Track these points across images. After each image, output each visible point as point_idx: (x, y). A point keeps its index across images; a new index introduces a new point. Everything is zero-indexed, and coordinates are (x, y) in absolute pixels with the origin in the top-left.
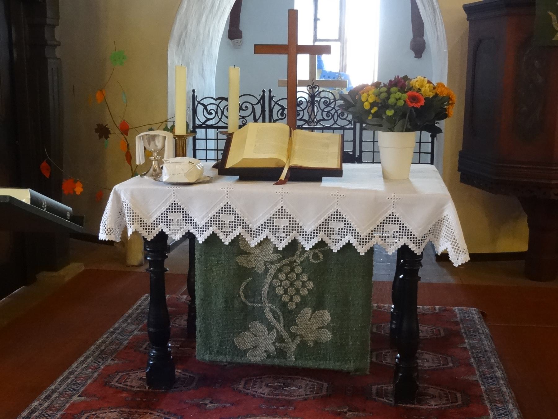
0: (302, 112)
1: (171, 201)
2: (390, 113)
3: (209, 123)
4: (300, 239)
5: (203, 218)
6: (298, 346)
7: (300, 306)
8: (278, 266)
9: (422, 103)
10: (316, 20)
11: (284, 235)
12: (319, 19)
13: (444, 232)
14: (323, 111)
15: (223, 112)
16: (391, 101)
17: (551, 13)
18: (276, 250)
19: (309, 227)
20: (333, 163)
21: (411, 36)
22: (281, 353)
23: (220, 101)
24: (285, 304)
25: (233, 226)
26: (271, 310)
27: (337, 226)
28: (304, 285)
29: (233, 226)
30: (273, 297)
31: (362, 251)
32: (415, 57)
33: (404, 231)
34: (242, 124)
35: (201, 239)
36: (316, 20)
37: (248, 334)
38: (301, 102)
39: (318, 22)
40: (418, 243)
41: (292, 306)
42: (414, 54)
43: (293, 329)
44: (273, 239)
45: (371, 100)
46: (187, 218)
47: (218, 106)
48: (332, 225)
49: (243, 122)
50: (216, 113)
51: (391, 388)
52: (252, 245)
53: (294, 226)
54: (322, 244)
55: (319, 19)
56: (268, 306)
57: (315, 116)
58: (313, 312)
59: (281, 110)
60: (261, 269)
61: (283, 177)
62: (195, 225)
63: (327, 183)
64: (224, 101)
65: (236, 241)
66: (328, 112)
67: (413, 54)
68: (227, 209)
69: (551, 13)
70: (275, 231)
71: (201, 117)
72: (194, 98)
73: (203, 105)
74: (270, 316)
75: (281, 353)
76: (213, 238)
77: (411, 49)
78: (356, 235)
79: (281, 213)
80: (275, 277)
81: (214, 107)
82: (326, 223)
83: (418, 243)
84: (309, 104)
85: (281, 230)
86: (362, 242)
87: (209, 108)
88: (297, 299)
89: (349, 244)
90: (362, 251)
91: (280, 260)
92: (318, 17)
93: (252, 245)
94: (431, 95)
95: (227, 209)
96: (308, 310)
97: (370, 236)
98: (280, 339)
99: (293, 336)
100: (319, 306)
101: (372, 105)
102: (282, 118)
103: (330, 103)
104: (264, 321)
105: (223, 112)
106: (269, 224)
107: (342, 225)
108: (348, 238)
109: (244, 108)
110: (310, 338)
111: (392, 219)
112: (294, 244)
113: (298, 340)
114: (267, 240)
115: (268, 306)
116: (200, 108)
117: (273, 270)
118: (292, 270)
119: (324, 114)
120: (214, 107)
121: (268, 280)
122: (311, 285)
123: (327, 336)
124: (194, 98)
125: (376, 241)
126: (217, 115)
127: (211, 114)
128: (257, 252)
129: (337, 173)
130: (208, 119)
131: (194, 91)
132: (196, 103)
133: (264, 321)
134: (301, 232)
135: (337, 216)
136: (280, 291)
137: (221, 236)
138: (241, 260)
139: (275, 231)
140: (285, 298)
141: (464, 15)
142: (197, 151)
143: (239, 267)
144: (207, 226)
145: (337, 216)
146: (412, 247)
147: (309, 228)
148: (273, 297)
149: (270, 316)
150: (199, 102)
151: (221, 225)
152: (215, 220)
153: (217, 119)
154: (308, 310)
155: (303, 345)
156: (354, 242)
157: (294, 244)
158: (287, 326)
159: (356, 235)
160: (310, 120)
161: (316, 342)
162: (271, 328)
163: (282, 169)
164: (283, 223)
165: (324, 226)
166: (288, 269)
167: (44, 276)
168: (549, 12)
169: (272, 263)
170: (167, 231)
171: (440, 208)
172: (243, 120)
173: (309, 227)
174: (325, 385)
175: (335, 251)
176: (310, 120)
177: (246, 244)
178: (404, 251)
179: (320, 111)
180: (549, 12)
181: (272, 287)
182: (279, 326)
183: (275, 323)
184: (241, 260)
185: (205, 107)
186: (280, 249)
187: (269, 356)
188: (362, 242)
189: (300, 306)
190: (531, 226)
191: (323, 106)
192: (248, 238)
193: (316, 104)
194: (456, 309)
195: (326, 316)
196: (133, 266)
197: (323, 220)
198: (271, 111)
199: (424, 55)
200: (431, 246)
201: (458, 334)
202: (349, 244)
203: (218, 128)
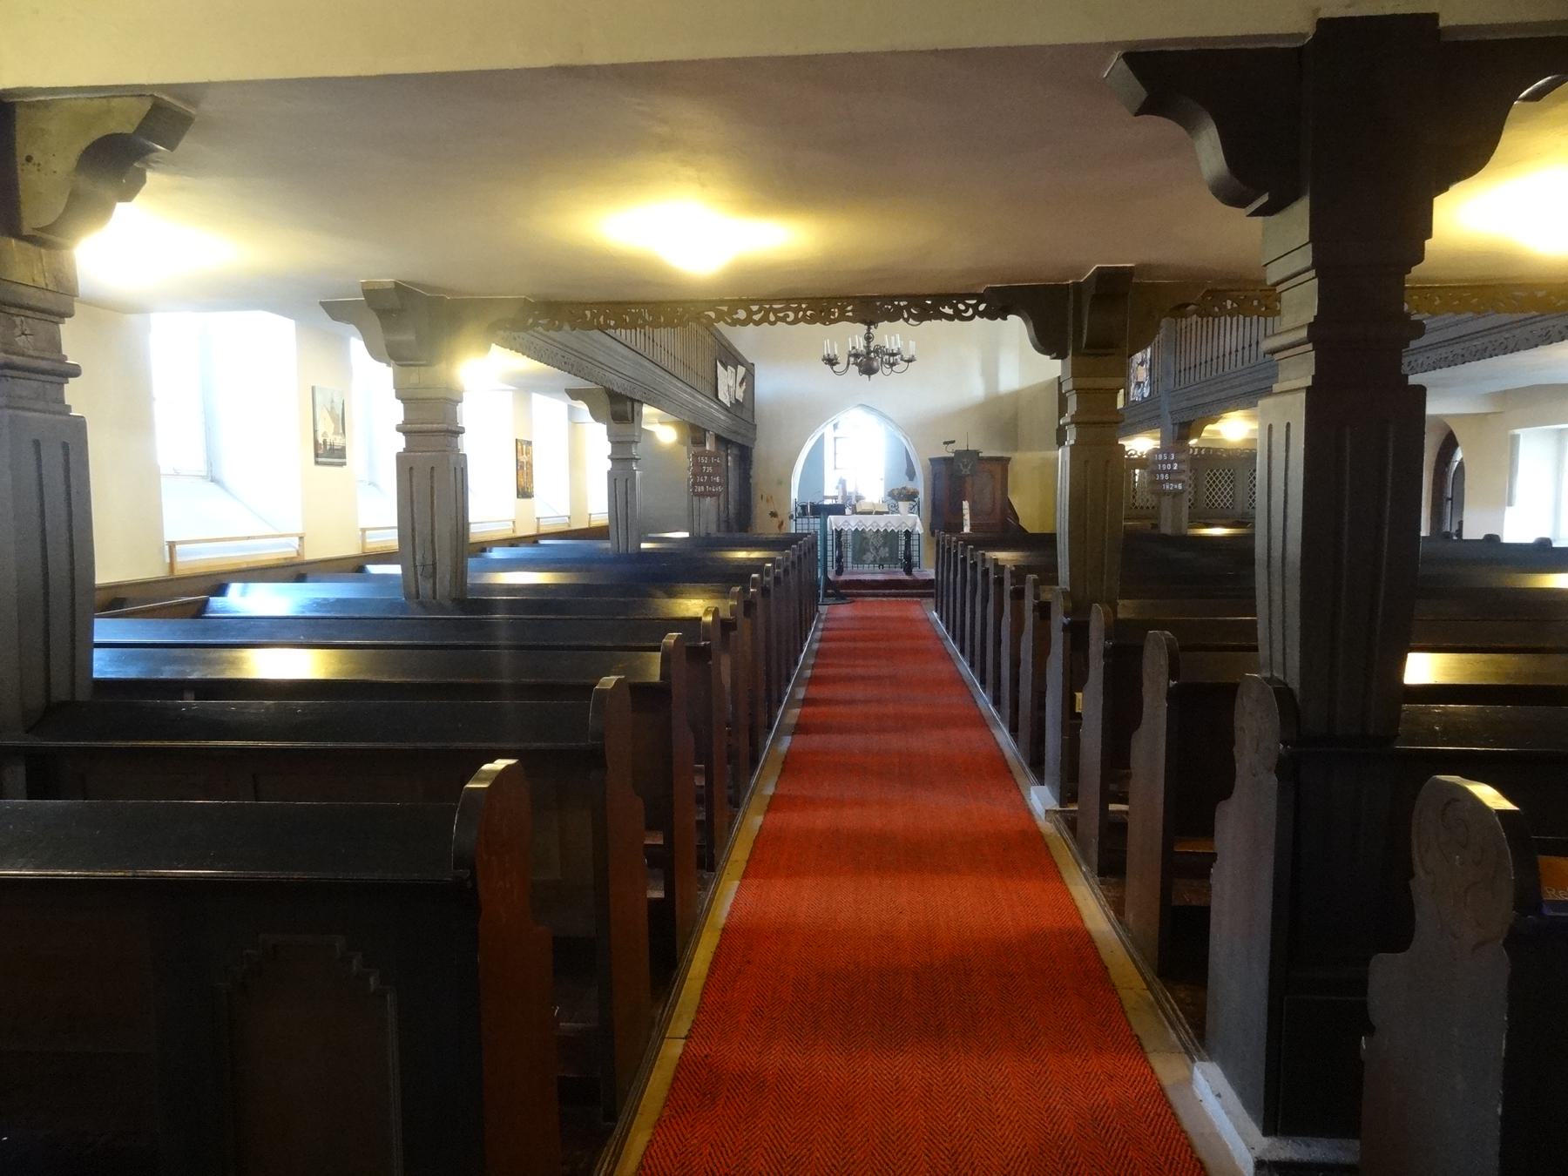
10: (835, 454)
31: (896, 531)
33: (907, 526)
36: (835, 454)
46: (849, 524)
53: (878, 525)
54: (886, 530)
65: (863, 530)
90: (896, 531)
95: (860, 521)
106: (871, 525)
108: (893, 528)
123: (887, 555)
125: (900, 528)
135: (889, 522)
141: (929, 463)
145: (889, 522)
154: (882, 548)
155: (881, 558)
165: (886, 525)
173: (882, 524)
178: (907, 530)
195: (887, 549)
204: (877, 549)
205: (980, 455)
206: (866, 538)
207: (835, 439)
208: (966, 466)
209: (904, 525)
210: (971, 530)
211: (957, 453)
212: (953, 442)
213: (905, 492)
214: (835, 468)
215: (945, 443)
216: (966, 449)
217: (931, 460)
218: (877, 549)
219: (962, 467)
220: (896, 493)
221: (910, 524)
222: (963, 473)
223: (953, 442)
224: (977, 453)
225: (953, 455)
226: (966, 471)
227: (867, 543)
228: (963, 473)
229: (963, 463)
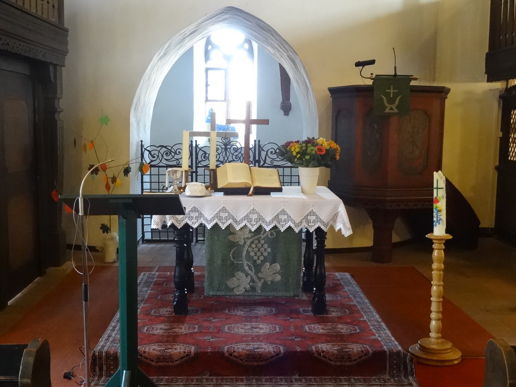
0: (219, 155)
1: (192, 206)
2: (308, 157)
3: (152, 163)
4: (264, 226)
5: (210, 215)
6: (262, 284)
7: (263, 262)
8: (252, 240)
9: (324, 152)
10: (207, 85)
11: (255, 223)
12: (209, 85)
13: (339, 219)
14: (233, 154)
15: (162, 156)
16: (309, 151)
17: (383, 97)
18: (250, 231)
19: (268, 218)
20: (277, 185)
21: (280, 99)
22: (253, 289)
23: (160, 148)
24: (255, 261)
25: (227, 219)
26: (248, 265)
27: (283, 217)
28: (265, 250)
29: (227, 219)
30: (249, 257)
31: (297, 230)
32: (284, 115)
33: (318, 219)
34: (176, 164)
35: (209, 227)
36: (207, 85)
37: (234, 278)
38: (218, 149)
39: (209, 87)
40: (326, 225)
41: (259, 262)
42: (283, 112)
43: (260, 275)
44: (249, 225)
45: (297, 150)
46: (201, 215)
47: (159, 152)
48: (281, 217)
49: (177, 163)
50: (158, 156)
51: (311, 309)
52: (237, 229)
53: (260, 218)
54: (275, 227)
55: (209, 85)
56: (245, 262)
57: (228, 158)
58: (271, 265)
59: (204, 155)
60: (241, 243)
61: (251, 192)
62: (206, 219)
63: (273, 195)
64: (163, 148)
65: (229, 227)
66: (236, 155)
67: (282, 113)
68: (224, 210)
69: (383, 97)
70: (250, 221)
71: (147, 159)
72: (142, 146)
73: (148, 150)
74: (247, 268)
75: (253, 289)
76: (216, 226)
77: (281, 109)
78: (294, 222)
79: (253, 211)
80: (250, 246)
81: (157, 153)
82: (277, 216)
83: (326, 225)
84: (223, 150)
85: (253, 221)
86: (297, 225)
87: (152, 153)
88: (262, 258)
89: (290, 227)
90: (297, 230)
91: (252, 237)
92: (209, 84)
93: (237, 229)
94: (328, 148)
95: (224, 210)
96: (268, 264)
97: (301, 222)
98: (252, 281)
99: (260, 279)
100: (273, 262)
101: (297, 153)
102: (205, 159)
103: (238, 150)
104: (243, 271)
105: (162, 156)
106: (247, 217)
107: (286, 217)
108: (290, 224)
109: (178, 153)
110: (269, 279)
111: (312, 213)
112: (260, 227)
113: (262, 281)
114: (245, 226)
115: (245, 262)
116: (146, 154)
117: (248, 243)
118: (259, 242)
119: (234, 157)
120: (157, 153)
121: (246, 248)
122: (269, 250)
123: (278, 278)
124: (142, 146)
126: (176, 159)
127: (154, 157)
128: (240, 233)
129: (279, 190)
130: (152, 161)
131: (142, 141)
132: (144, 149)
133: (243, 271)
134: (264, 221)
135: (283, 212)
136: (252, 254)
137: (220, 225)
138: (231, 238)
139: (250, 221)
140: (255, 258)
142: (144, 183)
143: (230, 241)
144: (212, 219)
145: (283, 212)
146: (323, 227)
147: (268, 219)
148: (249, 257)
149: (247, 268)
150: (145, 149)
151: (220, 219)
152: (217, 216)
153: (158, 161)
154: (268, 264)
155: (265, 282)
156: (292, 226)
157: (260, 228)
158: (256, 273)
159: (294, 222)
160: (224, 161)
161: (272, 282)
162: (247, 275)
163: (249, 188)
164: (254, 217)
165: (276, 218)
166: (256, 242)
167: (51, 270)
168: (382, 96)
169: (248, 238)
170: (190, 223)
171: (336, 207)
172: (177, 161)
173: (268, 218)
174: (274, 309)
175: (282, 231)
176: (224, 161)
177: (234, 228)
179: (231, 155)
180: (382, 96)
181: (248, 252)
182: (252, 273)
183: (249, 272)
184: (231, 238)
185: (150, 152)
186: (253, 231)
187: (246, 291)
188: (297, 225)
189: (263, 262)
190: (374, 227)
191: (232, 151)
192: (235, 225)
193: (229, 150)
194: (337, 274)
196: (109, 263)
197: (276, 214)
198: (197, 155)
199: (291, 113)
200: (332, 228)
201: (340, 285)
202: (290, 227)
203: (159, 167)
204: (258, 268)
205: (413, 83)
206: (232, 245)
207: (207, 70)
208: (391, 101)
209: (312, 218)
210: (447, 231)
211: (378, 79)
212: (372, 62)
213: (312, 150)
214: (207, 100)
215: (358, 64)
216: (393, 74)
217: (333, 91)
218: (258, 268)
219: (385, 102)
220: (295, 150)
221: (324, 216)
222: (387, 111)
223: (372, 62)
224: (408, 78)
225: (370, 82)
226: (391, 108)
227: (237, 255)
228: (387, 111)
229: (387, 95)
